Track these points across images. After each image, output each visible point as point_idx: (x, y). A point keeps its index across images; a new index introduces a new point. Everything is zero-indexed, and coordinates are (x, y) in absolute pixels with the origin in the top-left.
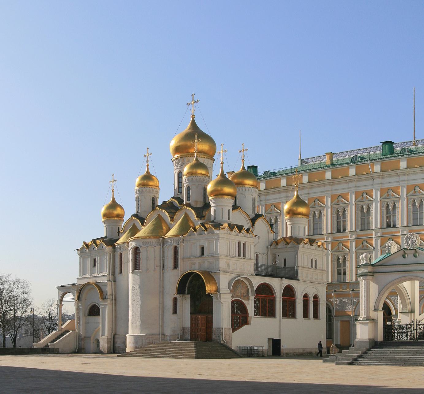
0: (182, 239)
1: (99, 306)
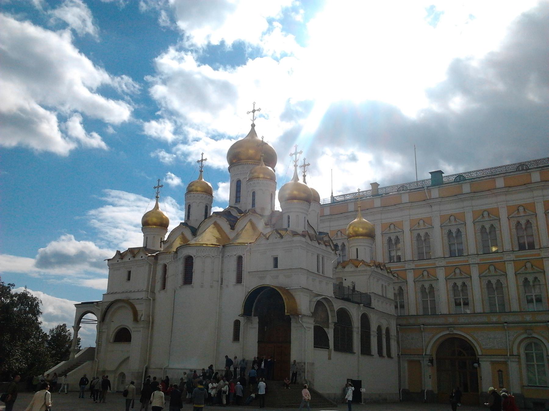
0: (249, 248)
1: (131, 330)
